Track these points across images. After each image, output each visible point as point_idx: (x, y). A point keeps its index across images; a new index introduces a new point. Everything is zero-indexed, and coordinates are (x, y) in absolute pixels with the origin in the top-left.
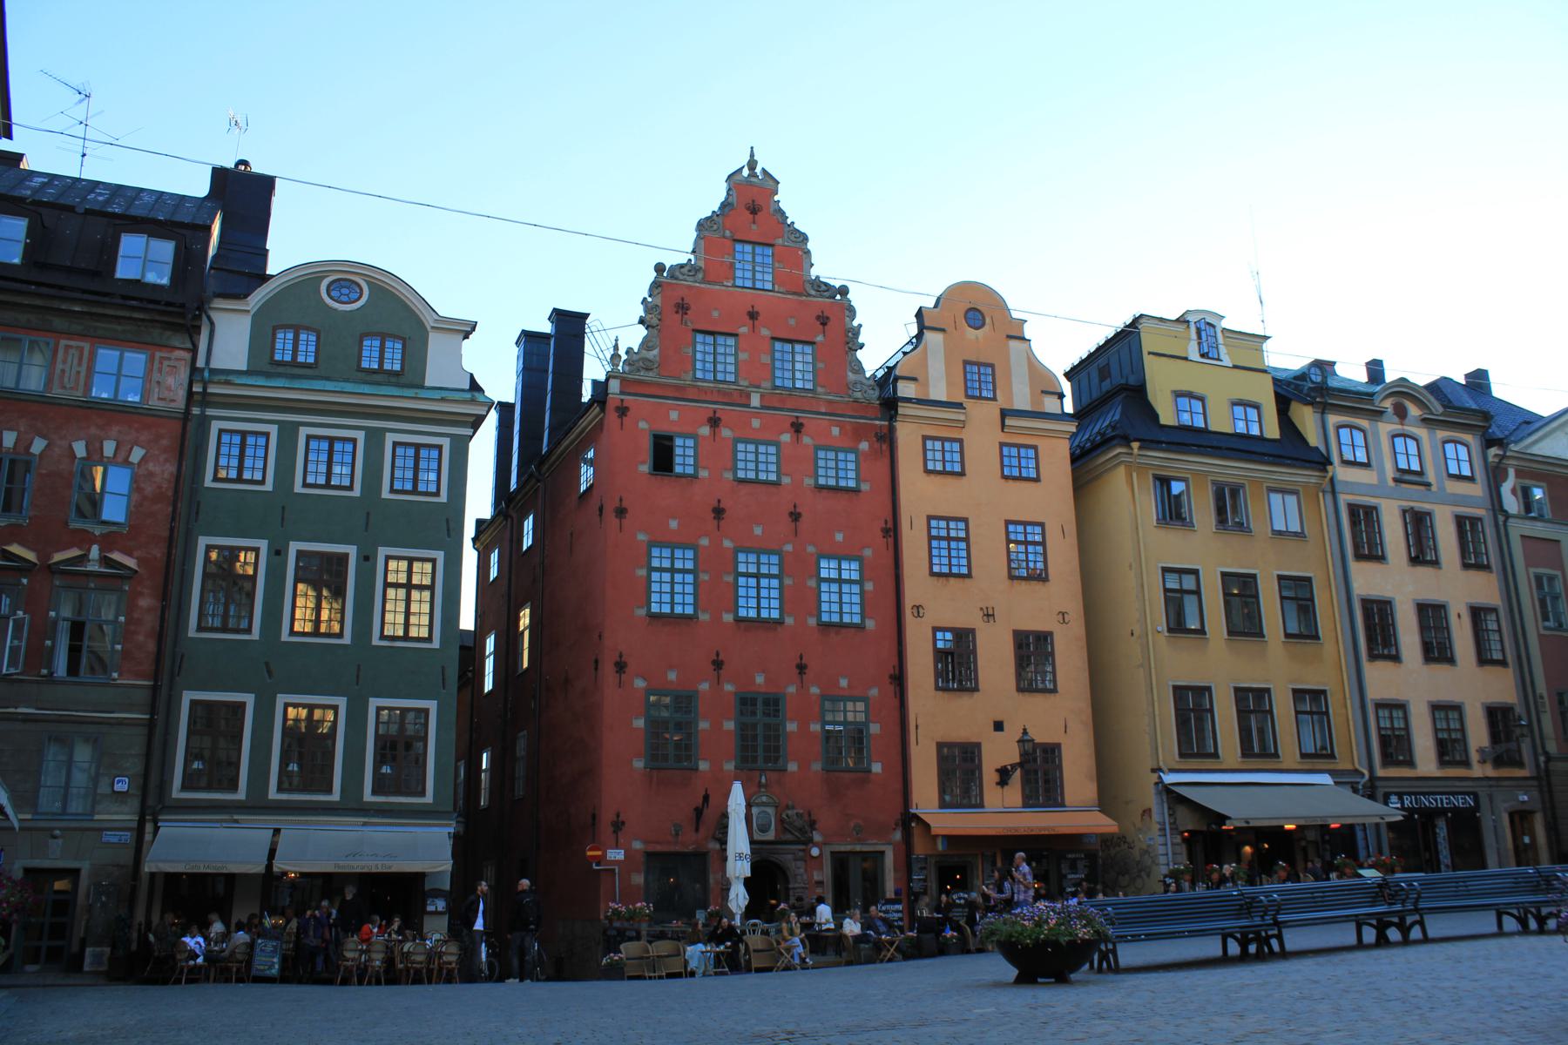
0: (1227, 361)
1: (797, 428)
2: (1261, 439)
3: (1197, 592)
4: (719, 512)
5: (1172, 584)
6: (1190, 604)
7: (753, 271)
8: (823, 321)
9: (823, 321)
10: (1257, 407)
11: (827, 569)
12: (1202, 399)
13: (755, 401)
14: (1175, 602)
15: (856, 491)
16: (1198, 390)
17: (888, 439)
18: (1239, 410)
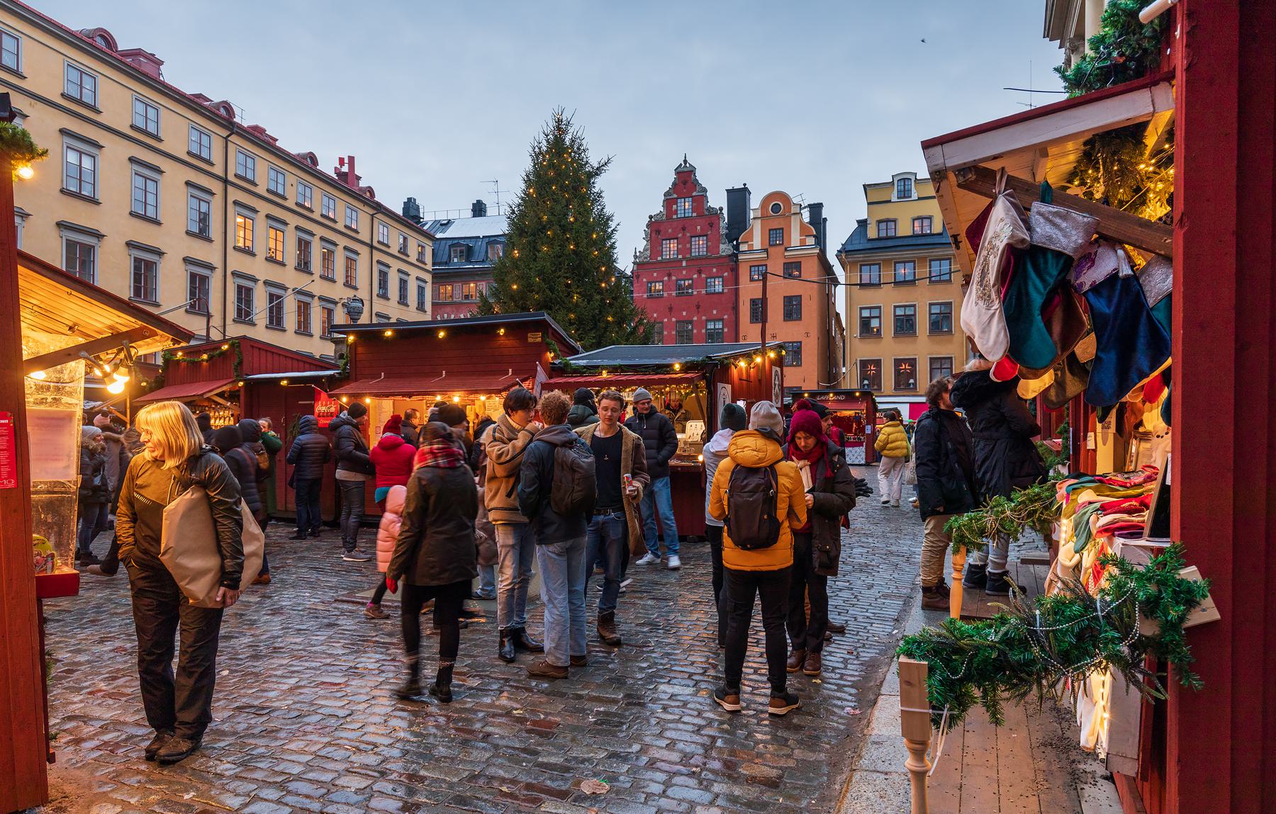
0: (915, 196)
1: (699, 272)
2: (931, 235)
3: (879, 317)
4: (671, 309)
5: (866, 314)
6: (874, 323)
7: (685, 207)
8: (711, 225)
9: (711, 225)
10: (930, 218)
11: (711, 326)
12: (894, 221)
13: (684, 264)
14: (865, 323)
15: (722, 293)
16: (892, 216)
17: (735, 270)
18: (917, 223)
